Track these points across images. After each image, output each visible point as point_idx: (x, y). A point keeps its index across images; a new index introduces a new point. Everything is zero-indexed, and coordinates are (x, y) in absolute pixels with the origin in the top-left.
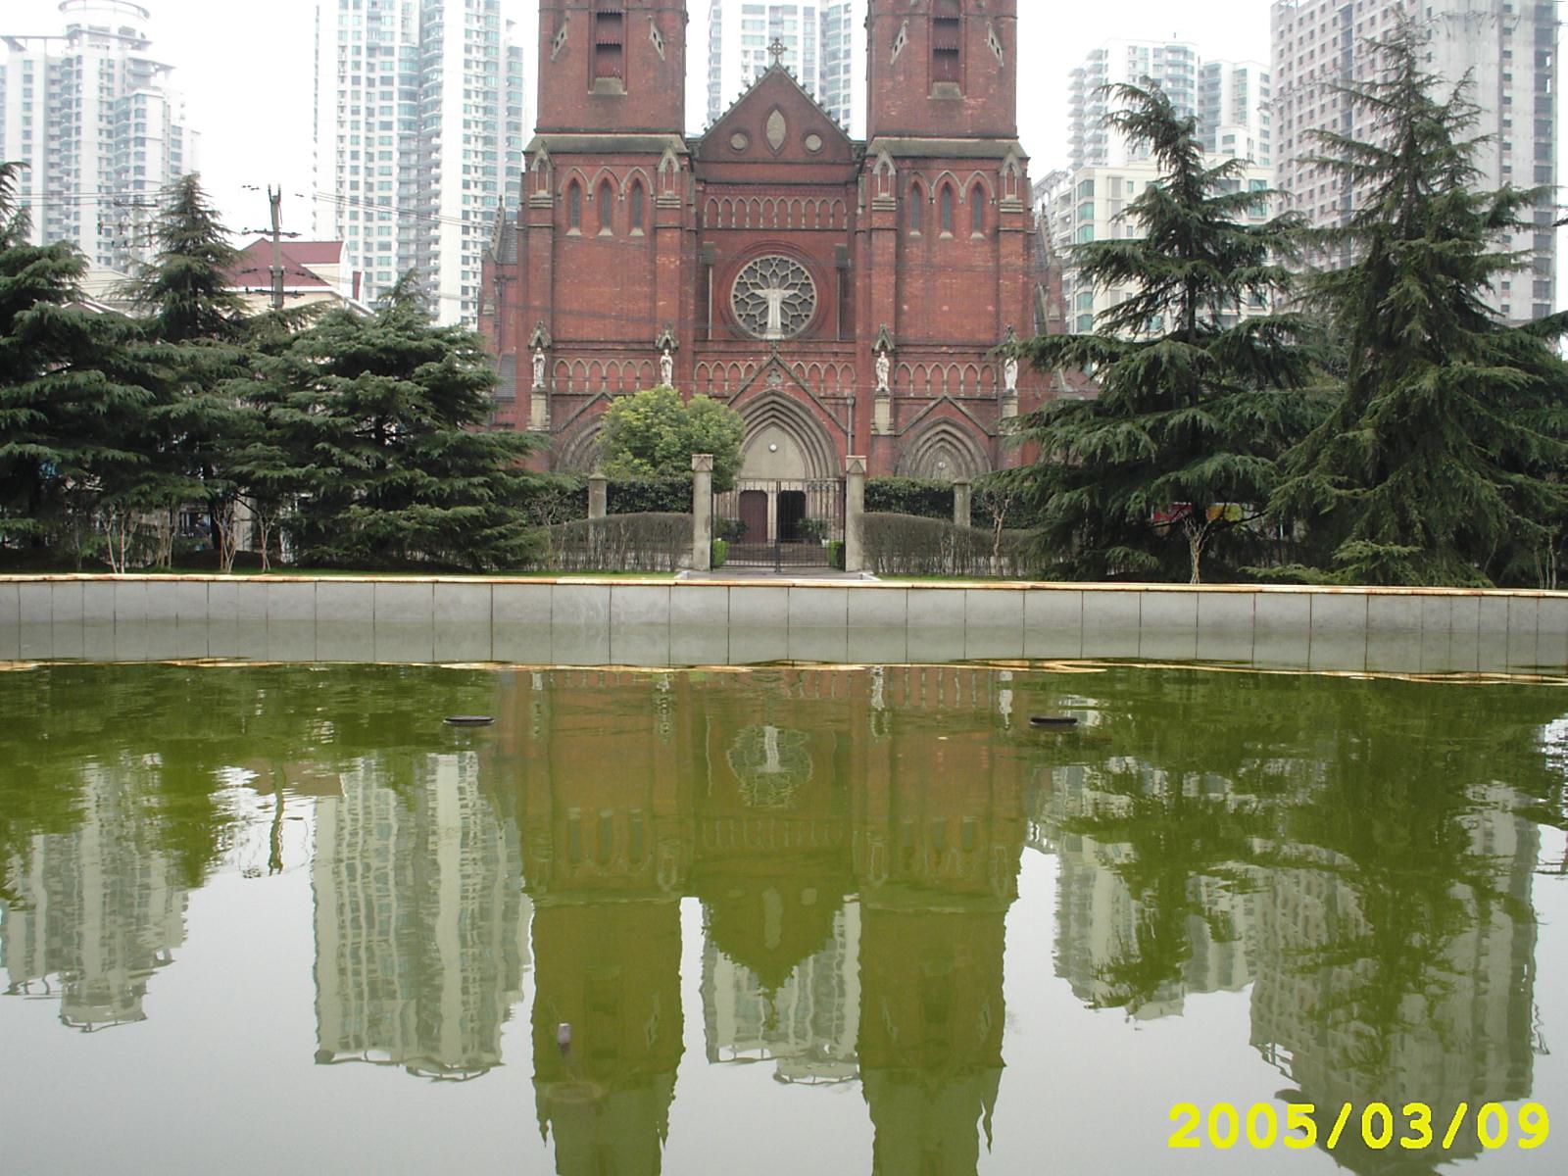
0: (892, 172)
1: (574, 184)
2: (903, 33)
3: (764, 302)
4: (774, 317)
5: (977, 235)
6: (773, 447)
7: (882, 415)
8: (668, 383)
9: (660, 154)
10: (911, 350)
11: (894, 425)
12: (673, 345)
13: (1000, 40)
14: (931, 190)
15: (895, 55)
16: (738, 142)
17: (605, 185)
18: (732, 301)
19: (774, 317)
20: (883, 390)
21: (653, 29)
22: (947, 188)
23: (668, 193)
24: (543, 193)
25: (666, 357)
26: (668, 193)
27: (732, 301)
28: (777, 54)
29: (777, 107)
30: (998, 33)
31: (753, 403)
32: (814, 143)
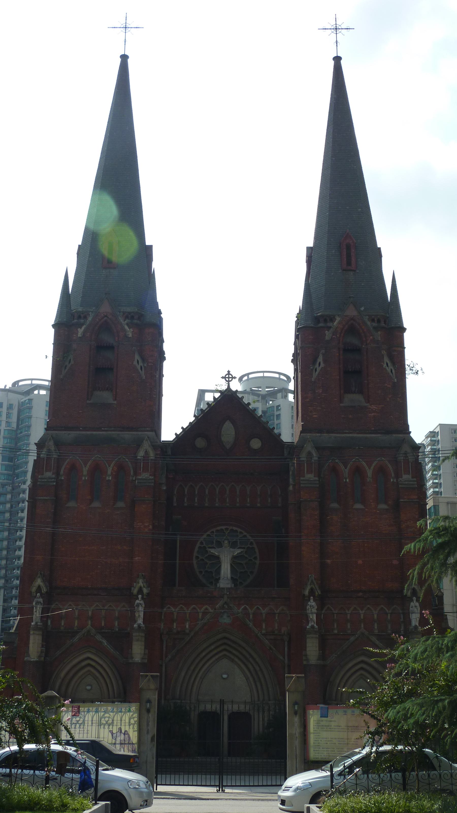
1: (73, 468)
2: (320, 359)
3: (218, 558)
4: (226, 569)
5: (383, 506)
6: (225, 676)
7: (312, 648)
8: (140, 621)
11: (323, 656)
12: (145, 591)
13: (394, 364)
14: (345, 472)
15: (315, 375)
16: (200, 443)
17: (97, 469)
19: (226, 569)
20: (313, 627)
21: (137, 357)
22: (358, 471)
23: (145, 475)
24: (48, 474)
26: (145, 475)
30: (391, 358)
32: (256, 444)
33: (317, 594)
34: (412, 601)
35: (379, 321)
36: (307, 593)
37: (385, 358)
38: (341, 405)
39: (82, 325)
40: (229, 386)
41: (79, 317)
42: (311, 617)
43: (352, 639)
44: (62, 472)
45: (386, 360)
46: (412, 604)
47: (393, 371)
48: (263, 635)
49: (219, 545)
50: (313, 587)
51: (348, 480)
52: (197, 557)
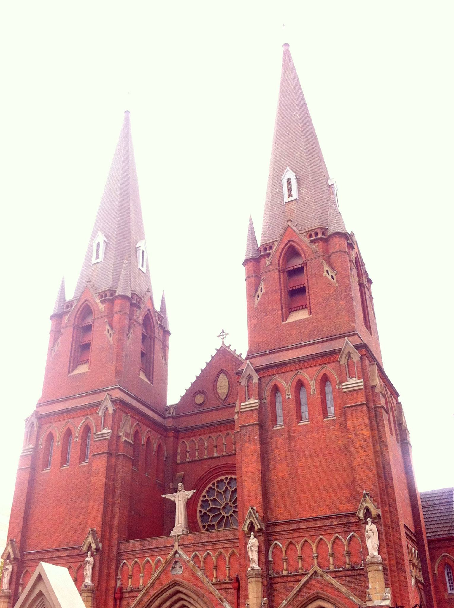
0: (255, 379)
9: (100, 403)
10: (284, 527)
13: (333, 269)
18: (198, 515)
21: (108, 327)
25: (90, 559)
27: (198, 515)
28: (223, 338)
29: (222, 371)
31: (161, 593)
33: (256, 528)
34: (366, 523)
35: (316, 234)
36: (246, 529)
37: (324, 266)
38: (284, 323)
39: (69, 311)
40: (223, 343)
41: (68, 307)
42: (251, 557)
43: (305, 579)
44: (40, 443)
45: (326, 267)
46: (368, 527)
47: (334, 277)
48: (213, 584)
49: (175, 490)
50: (253, 520)
51: (290, 397)
52: (201, 512)
